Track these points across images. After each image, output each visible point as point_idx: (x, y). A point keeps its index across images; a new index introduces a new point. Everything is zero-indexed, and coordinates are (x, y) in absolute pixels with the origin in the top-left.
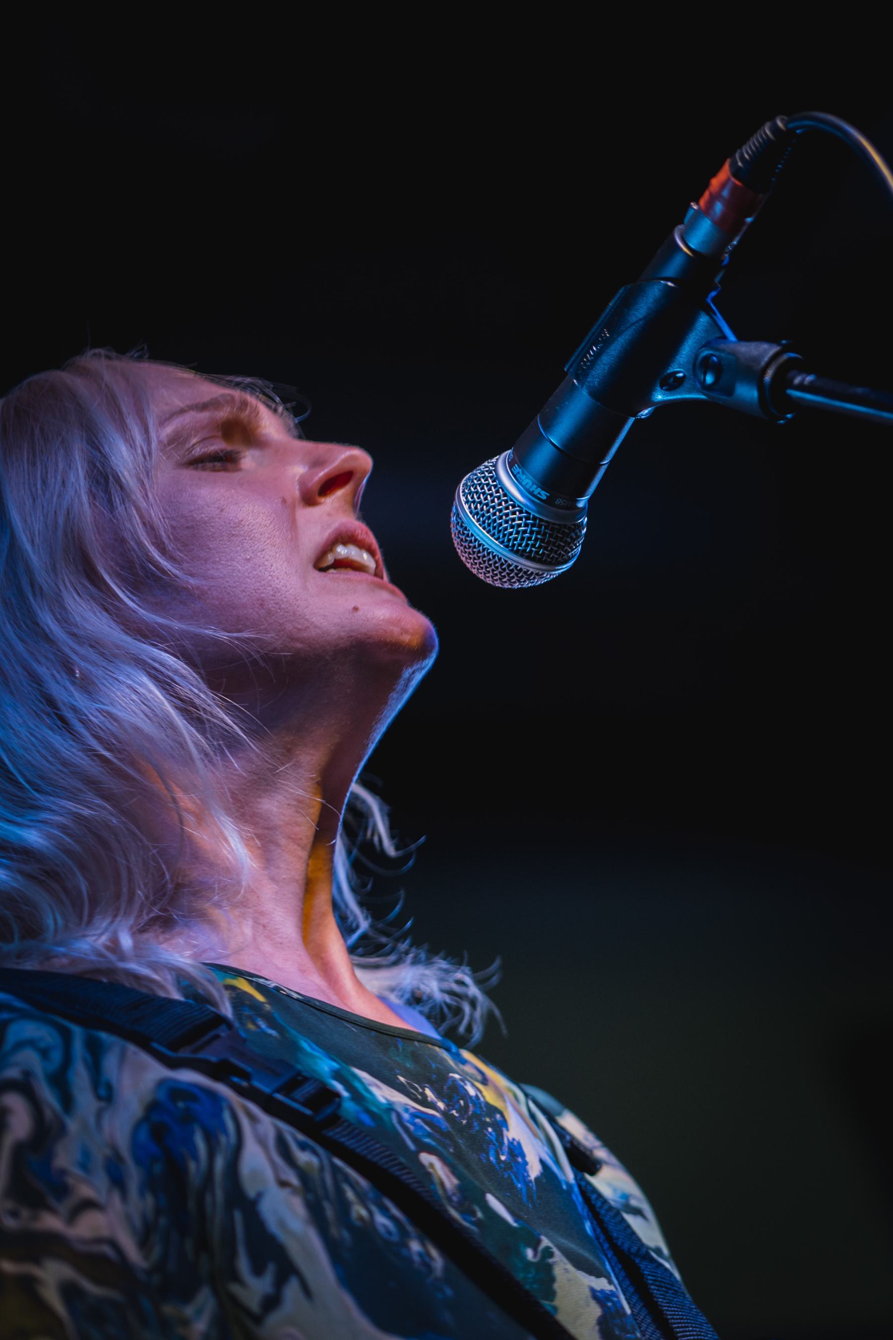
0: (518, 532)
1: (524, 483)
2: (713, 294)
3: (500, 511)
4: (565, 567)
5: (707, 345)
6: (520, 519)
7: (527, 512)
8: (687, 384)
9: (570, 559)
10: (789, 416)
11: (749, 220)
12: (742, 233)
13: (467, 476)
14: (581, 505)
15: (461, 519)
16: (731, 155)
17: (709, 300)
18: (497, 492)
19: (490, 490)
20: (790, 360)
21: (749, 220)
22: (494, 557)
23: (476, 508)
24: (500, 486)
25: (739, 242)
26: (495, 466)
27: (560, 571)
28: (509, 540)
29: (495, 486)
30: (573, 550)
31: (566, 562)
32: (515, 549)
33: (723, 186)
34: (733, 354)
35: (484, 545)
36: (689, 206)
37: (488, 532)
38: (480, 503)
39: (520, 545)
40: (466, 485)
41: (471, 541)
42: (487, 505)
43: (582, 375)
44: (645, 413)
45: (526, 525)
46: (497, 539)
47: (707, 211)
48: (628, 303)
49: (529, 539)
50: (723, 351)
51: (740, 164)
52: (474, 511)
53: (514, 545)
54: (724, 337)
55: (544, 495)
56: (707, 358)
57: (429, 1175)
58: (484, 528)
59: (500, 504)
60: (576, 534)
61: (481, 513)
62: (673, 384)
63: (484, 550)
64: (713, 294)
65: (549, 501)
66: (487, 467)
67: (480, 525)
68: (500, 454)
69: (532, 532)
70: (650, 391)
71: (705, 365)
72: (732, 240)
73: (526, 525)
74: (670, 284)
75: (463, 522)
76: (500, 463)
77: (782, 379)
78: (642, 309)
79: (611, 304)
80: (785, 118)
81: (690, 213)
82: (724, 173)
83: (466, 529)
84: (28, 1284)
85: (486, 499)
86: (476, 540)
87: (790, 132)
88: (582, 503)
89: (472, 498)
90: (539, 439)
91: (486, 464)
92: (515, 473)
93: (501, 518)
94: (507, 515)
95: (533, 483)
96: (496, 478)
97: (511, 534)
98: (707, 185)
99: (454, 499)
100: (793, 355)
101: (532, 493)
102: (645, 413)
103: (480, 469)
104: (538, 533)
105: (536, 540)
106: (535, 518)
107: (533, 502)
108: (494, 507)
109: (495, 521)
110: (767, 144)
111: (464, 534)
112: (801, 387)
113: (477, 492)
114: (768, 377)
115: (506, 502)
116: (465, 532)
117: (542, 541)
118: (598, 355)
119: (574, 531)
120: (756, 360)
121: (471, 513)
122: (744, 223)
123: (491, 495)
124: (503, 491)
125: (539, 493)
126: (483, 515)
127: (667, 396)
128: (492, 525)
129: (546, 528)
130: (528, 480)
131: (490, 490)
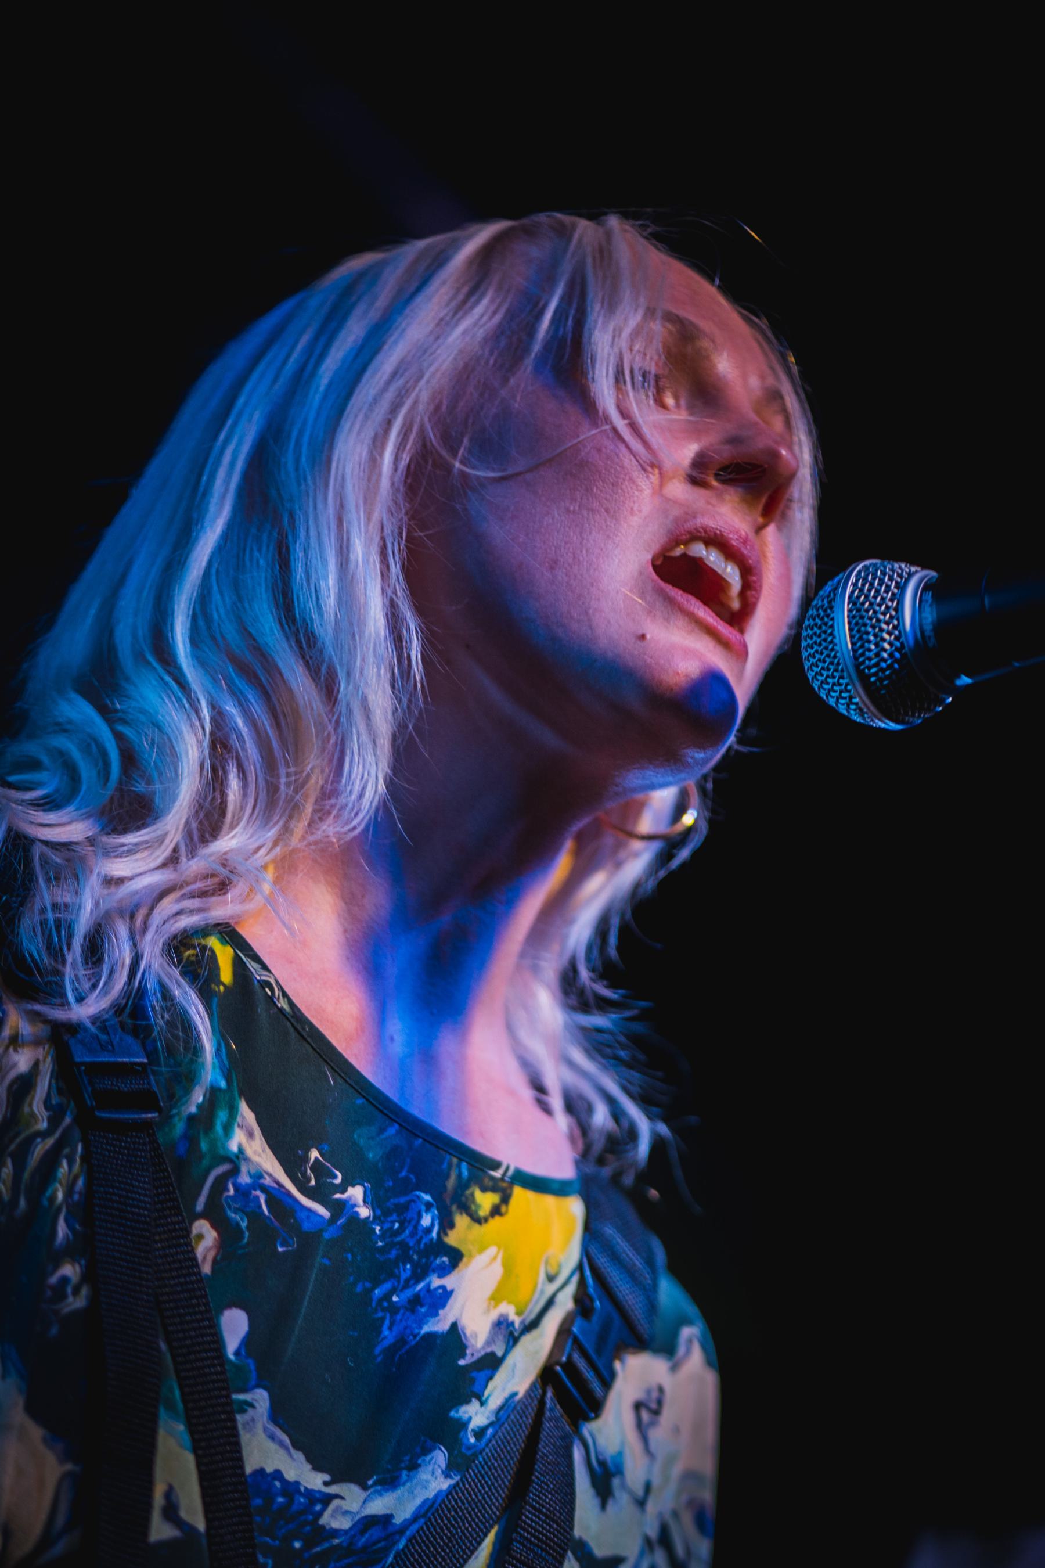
0: (877, 655)
1: (923, 615)
3: (879, 621)
4: (892, 726)
6: (891, 644)
7: (902, 644)
13: (874, 561)
15: (835, 595)
18: (892, 600)
23: (858, 597)
24: (899, 598)
26: (910, 575)
27: (883, 725)
28: (863, 654)
29: (893, 594)
30: (913, 716)
31: (897, 722)
32: (862, 667)
35: (834, 637)
37: (851, 630)
38: (867, 597)
39: (869, 668)
40: (866, 568)
42: (871, 604)
46: (853, 644)
49: (883, 670)
53: (863, 662)
58: (849, 623)
59: (884, 614)
66: (900, 568)
67: (848, 616)
69: (889, 667)
73: (891, 655)
75: (834, 599)
76: (918, 576)
83: (831, 608)
86: (832, 626)
91: (903, 566)
92: (923, 598)
93: (873, 627)
94: (881, 630)
95: (933, 623)
96: (902, 587)
97: (870, 650)
99: (844, 570)
101: (922, 632)
103: (893, 566)
105: (887, 677)
108: (875, 612)
109: (865, 625)
111: (825, 611)
113: (872, 585)
115: (891, 617)
116: (829, 611)
121: (850, 597)
124: (898, 603)
125: (929, 638)
126: (858, 610)
128: (859, 626)
130: (930, 616)
131: (886, 592)
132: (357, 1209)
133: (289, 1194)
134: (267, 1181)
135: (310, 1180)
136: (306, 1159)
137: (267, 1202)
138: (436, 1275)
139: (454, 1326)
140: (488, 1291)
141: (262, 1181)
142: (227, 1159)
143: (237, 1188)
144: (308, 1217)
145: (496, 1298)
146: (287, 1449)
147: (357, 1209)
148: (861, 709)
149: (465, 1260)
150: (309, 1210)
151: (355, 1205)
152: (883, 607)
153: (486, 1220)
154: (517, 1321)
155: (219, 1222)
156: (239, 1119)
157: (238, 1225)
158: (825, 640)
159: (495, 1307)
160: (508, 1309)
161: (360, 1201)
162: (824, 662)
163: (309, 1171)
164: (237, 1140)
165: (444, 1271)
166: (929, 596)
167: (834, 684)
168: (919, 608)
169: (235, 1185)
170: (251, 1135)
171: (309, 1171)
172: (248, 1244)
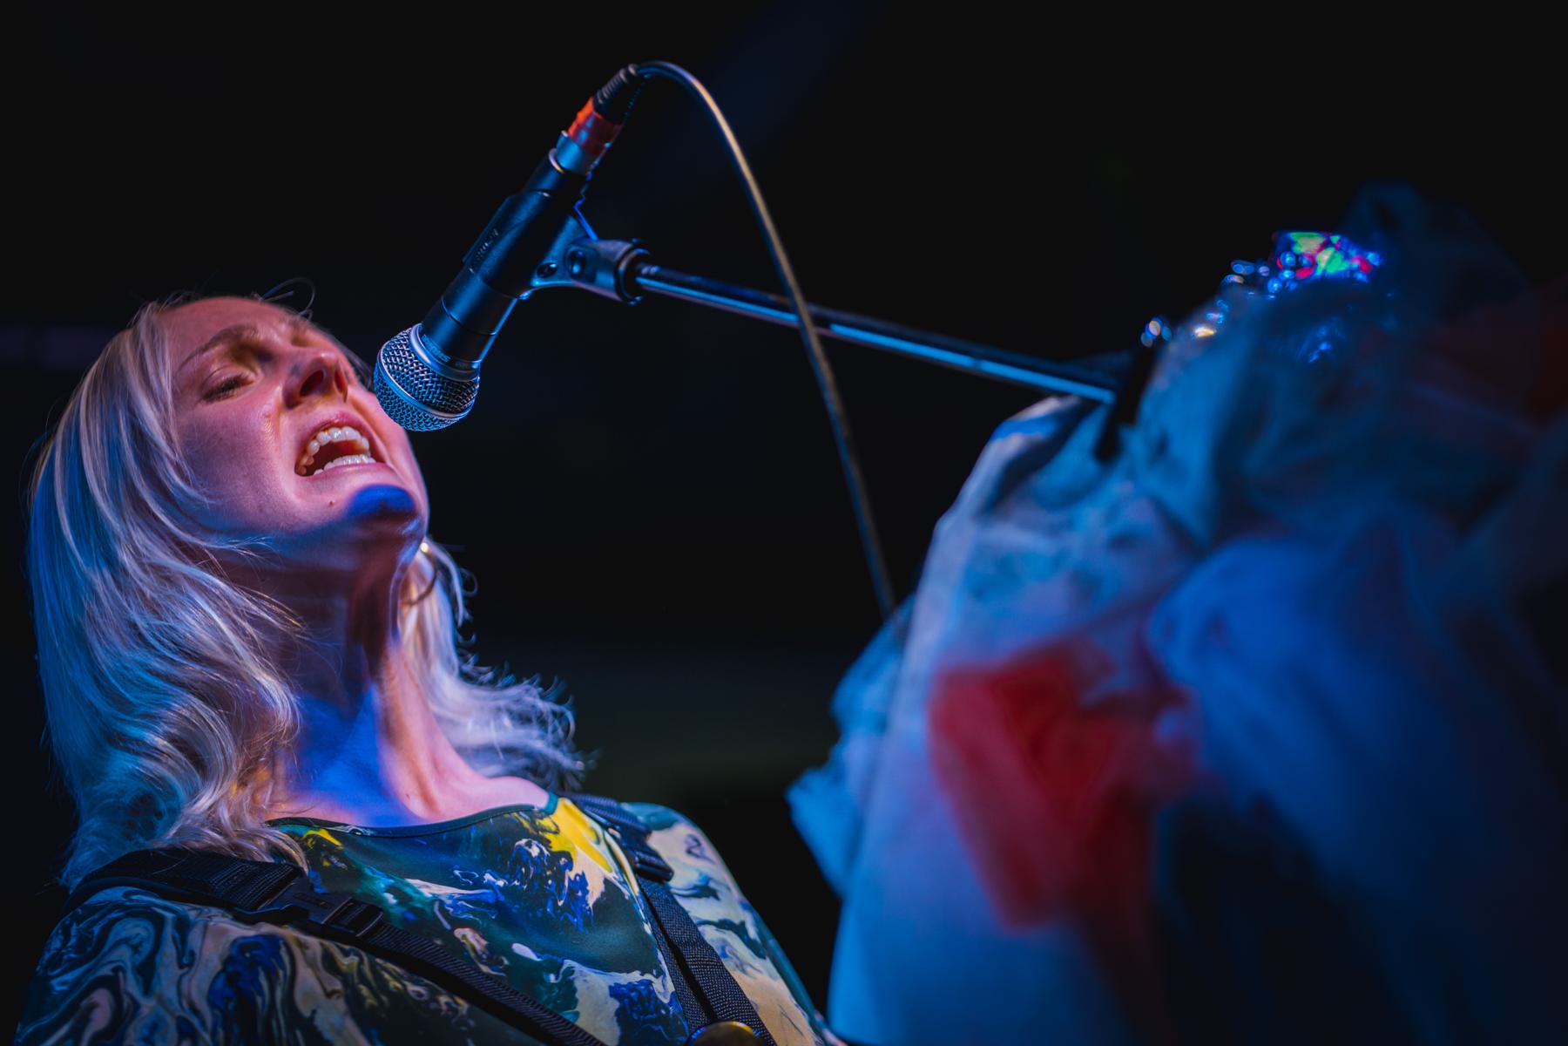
0: (426, 388)
1: (432, 348)
2: (580, 202)
3: (412, 371)
5: (574, 242)
6: (428, 377)
7: (433, 372)
8: (558, 273)
9: (466, 409)
10: (638, 298)
11: (607, 145)
12: (602, 155)
13: (386, 344)
14: (475, 367)
15: (382, 377)
16: (593, 94)
17: (576, 208)
18: (410, 356)
19: (404, 354)
20: (639, 255)
21: (607, 145)
22: (407, 406)
23: (393, 368)
24: (412, 351)
25: (601, 163)
26: (408, 335)
28: (419, 393)
29: (408, 351)
31: (463, 411)
33: (587, 118)
34: (595, 250)
36: (560, 134)
37: (403, 387)
38: (397, 364)
39: (428, 397)
40: (385, 350)
41: (389, 395)
42: (402, 366)
43: (477, 264)
44: (525, 295)
45: (432, 382)
46: (409, 393)
47: (574, 138)
48: (513, 209)
50: (586, 247)
51: (600, 101)
52: (392, 371)
54: (587, 236)
55: (446, 359)
56: (574, 254)
58: (400, 384)
59: (412, 365)
60: (471, 390)
61: (397, 372)
62: (548, 273)
63: (399, 401)
64: (580, 202)
65: (451, 364)
68: (412, 326)
69: (437, 388)
70: (529, 278)
71: (573, 258)
72: (594, 160)
73: (432, 382)
74: (546, 195)
76: (413, 333)
77: (633, 270)
78: (524, 214)
79: (500, 210)
80: (636, 66)
81: (561, 140)
82: (589, 108)
83: (385, 384)
85: (401, 361)
86: (393, 393)
87: (640, 77)
88: (476, 364)
89: (391, 360)
90: (441, 314)
91: (401, 333)
93: (412, 376)
94: (417, 374)
96: (409, 345)
97: (420, 388)
98: (574, 117)
99: (376, 361)
100: (641, 251)
101: (436, 357)
102: (525, 295)
104: (442, 388)
105: (440, 394)
106: (439, 377)
107: (437, 363)
108: (407, 368)
109: (408, 378)
110: (622, 85)
112: (648, 276)
113: (394, 356)
114: (623, 267)
115: (417, 363)
117: (445, 395)
118: (489, 249)
119: (469, 387)
120: (613, 254)
121: (389, 372)
122: (603, 147)
123: (405, 358)
126: (399, 374)
127: (546, 281)
129: (448, 384)
130: (434, 347)
131: (404, 354)
138: (567, 870)
148: (441, 421)
149: (572, 853)
152: (409, 362)
158: (395, 403)
162: (415, 416)
165: (570, 865)
166: (425, 338)
167: (418, 420)
168: (426, 348)
170: (427, 887)
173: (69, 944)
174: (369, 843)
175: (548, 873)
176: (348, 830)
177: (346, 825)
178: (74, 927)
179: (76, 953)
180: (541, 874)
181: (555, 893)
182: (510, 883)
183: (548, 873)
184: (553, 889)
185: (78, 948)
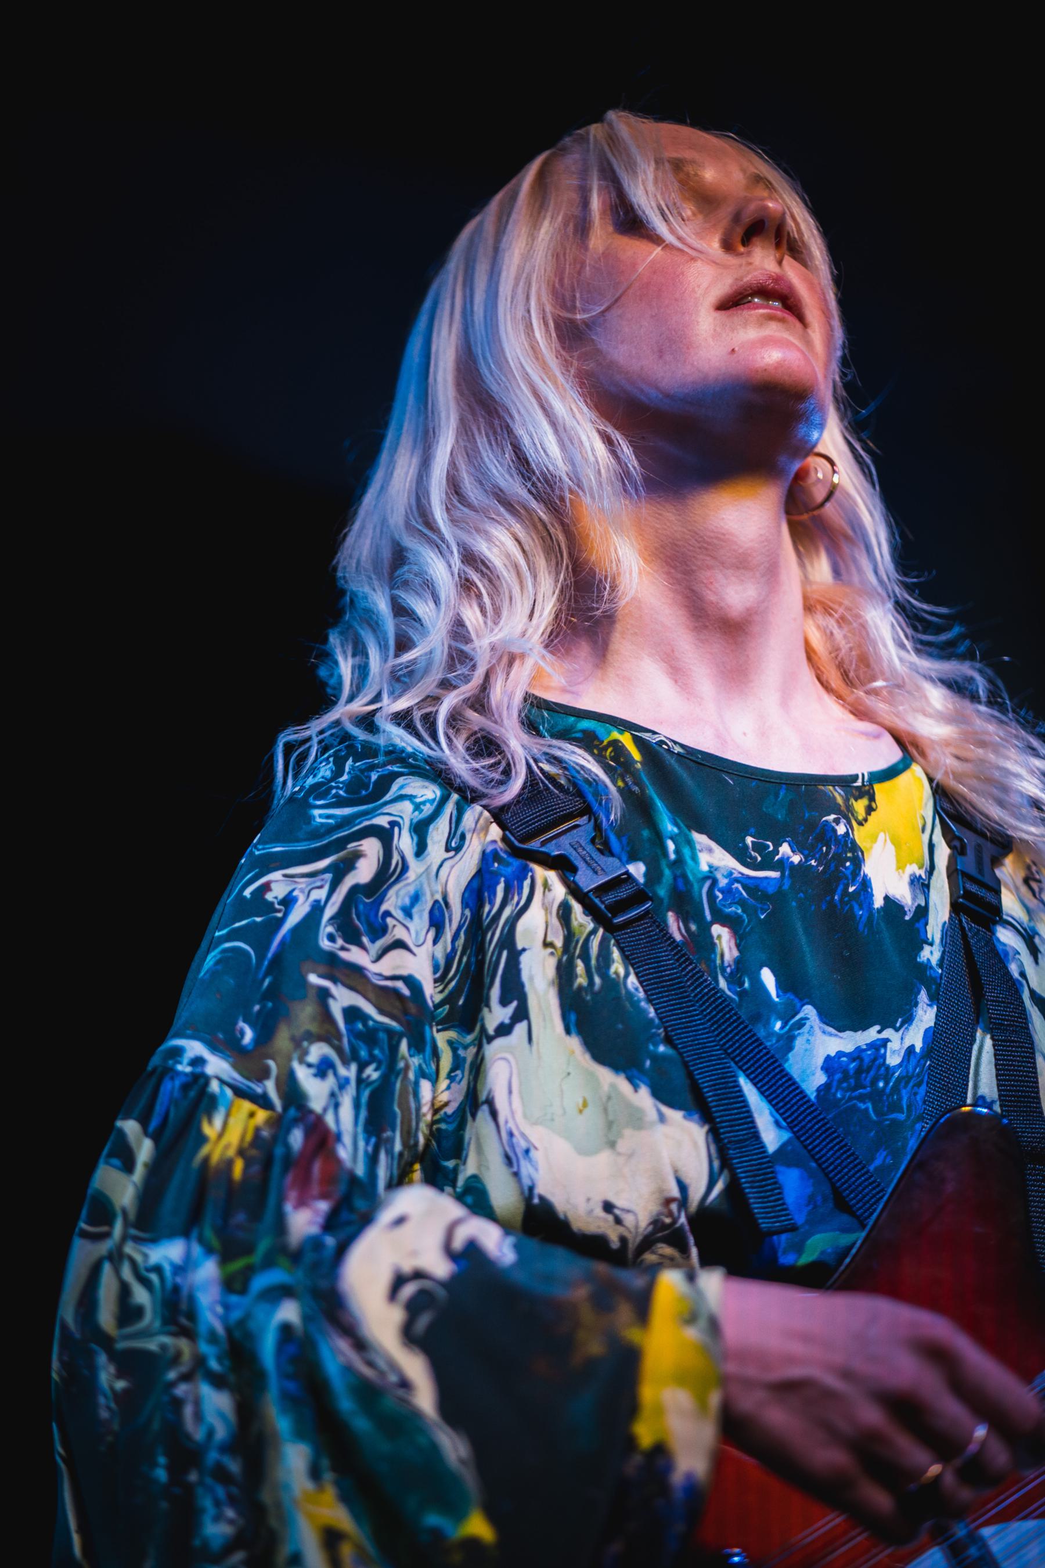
57: (713, 945)
84: (324, 995)
132: (791, 860)
133: (749, 877)
134: (736, 875)
135: (756, 858)
136: (746, 847)
137: (744, 889)
139: (887, 898)
140: (894, 866)
141: (734, 876)
142: (706, 878)
143: (722, 891)
144: (768, 883)
145: (900, 867)
146: (836, 1035)
147: (791, 860)
150: (766, 878)
151: (789, 858)
153: (866, 820)
154: (922, 873)
155: (721, 918)
156: (698, 847)
157: (736, 913)
159: (904, 872)
160: (914, 869)
161: (790, 853)
163: (753, 853)
164: (704, 861)
169: (719, 891)
170: (710, 850)
171: (753, 853)
172: (749, 922)
173: (341, 779)
174: (672, 761)
175: (849, 855)
176: (654, 739)
177: (654, 733)
178: (350, 762)
179: (345, 792)
180: (841, 854)
181: (850, 877)
182: (807, 860)
183: (849, 855)
184: (848, 872)
185: (349, 787)
